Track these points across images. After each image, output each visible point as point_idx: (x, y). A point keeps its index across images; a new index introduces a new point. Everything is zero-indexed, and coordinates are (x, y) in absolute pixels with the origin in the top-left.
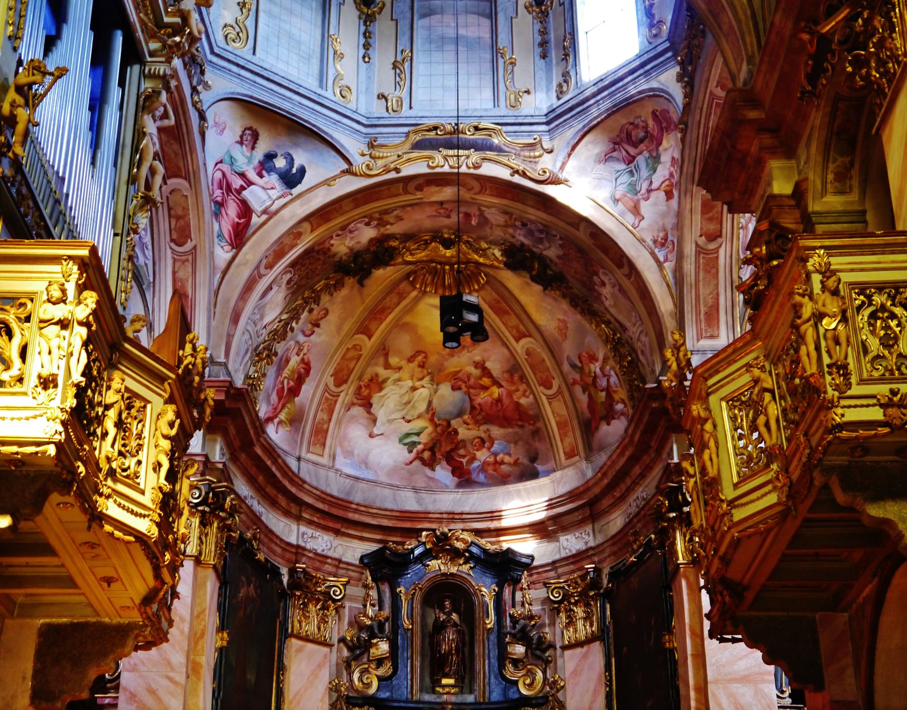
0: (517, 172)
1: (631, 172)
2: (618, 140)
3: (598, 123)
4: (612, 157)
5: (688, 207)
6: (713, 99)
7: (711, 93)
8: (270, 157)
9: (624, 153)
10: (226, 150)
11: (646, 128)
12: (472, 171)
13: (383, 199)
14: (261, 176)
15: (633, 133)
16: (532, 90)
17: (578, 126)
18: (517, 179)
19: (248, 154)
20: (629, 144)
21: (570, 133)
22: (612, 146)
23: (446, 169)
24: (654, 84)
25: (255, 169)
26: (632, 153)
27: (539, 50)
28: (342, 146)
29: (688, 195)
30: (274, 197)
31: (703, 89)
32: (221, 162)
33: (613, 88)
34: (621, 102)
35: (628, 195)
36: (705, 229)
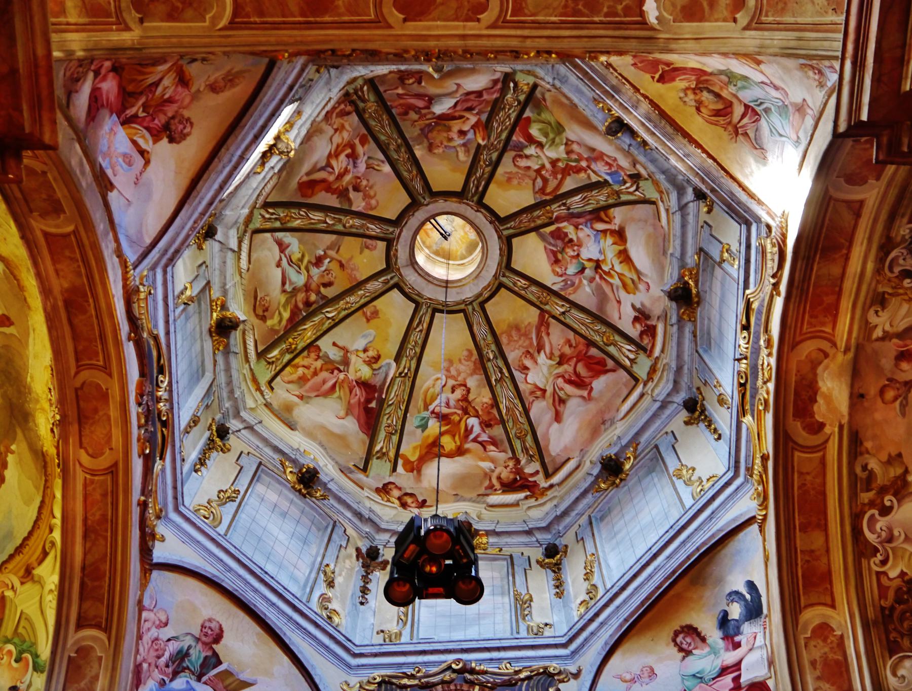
0: (776, 286)
1: (767, 110)
2: (730, 128)
4: (756, 139)
7: (493, 26)
8: (724, 621)
9: (745, 120)
10: (680, 679)
12: (775, 351)
13: (824, 484)
14: (737, 645)
15: (712, 107)
18: (783, 288)
19: (707, 650)
20: (731, 113)
22: (740, 138)
23: (771, 386)
25: (727, 650)
28: (734, 520)
30: (763, 642)
35: (791, 118)
36: (726, 13)
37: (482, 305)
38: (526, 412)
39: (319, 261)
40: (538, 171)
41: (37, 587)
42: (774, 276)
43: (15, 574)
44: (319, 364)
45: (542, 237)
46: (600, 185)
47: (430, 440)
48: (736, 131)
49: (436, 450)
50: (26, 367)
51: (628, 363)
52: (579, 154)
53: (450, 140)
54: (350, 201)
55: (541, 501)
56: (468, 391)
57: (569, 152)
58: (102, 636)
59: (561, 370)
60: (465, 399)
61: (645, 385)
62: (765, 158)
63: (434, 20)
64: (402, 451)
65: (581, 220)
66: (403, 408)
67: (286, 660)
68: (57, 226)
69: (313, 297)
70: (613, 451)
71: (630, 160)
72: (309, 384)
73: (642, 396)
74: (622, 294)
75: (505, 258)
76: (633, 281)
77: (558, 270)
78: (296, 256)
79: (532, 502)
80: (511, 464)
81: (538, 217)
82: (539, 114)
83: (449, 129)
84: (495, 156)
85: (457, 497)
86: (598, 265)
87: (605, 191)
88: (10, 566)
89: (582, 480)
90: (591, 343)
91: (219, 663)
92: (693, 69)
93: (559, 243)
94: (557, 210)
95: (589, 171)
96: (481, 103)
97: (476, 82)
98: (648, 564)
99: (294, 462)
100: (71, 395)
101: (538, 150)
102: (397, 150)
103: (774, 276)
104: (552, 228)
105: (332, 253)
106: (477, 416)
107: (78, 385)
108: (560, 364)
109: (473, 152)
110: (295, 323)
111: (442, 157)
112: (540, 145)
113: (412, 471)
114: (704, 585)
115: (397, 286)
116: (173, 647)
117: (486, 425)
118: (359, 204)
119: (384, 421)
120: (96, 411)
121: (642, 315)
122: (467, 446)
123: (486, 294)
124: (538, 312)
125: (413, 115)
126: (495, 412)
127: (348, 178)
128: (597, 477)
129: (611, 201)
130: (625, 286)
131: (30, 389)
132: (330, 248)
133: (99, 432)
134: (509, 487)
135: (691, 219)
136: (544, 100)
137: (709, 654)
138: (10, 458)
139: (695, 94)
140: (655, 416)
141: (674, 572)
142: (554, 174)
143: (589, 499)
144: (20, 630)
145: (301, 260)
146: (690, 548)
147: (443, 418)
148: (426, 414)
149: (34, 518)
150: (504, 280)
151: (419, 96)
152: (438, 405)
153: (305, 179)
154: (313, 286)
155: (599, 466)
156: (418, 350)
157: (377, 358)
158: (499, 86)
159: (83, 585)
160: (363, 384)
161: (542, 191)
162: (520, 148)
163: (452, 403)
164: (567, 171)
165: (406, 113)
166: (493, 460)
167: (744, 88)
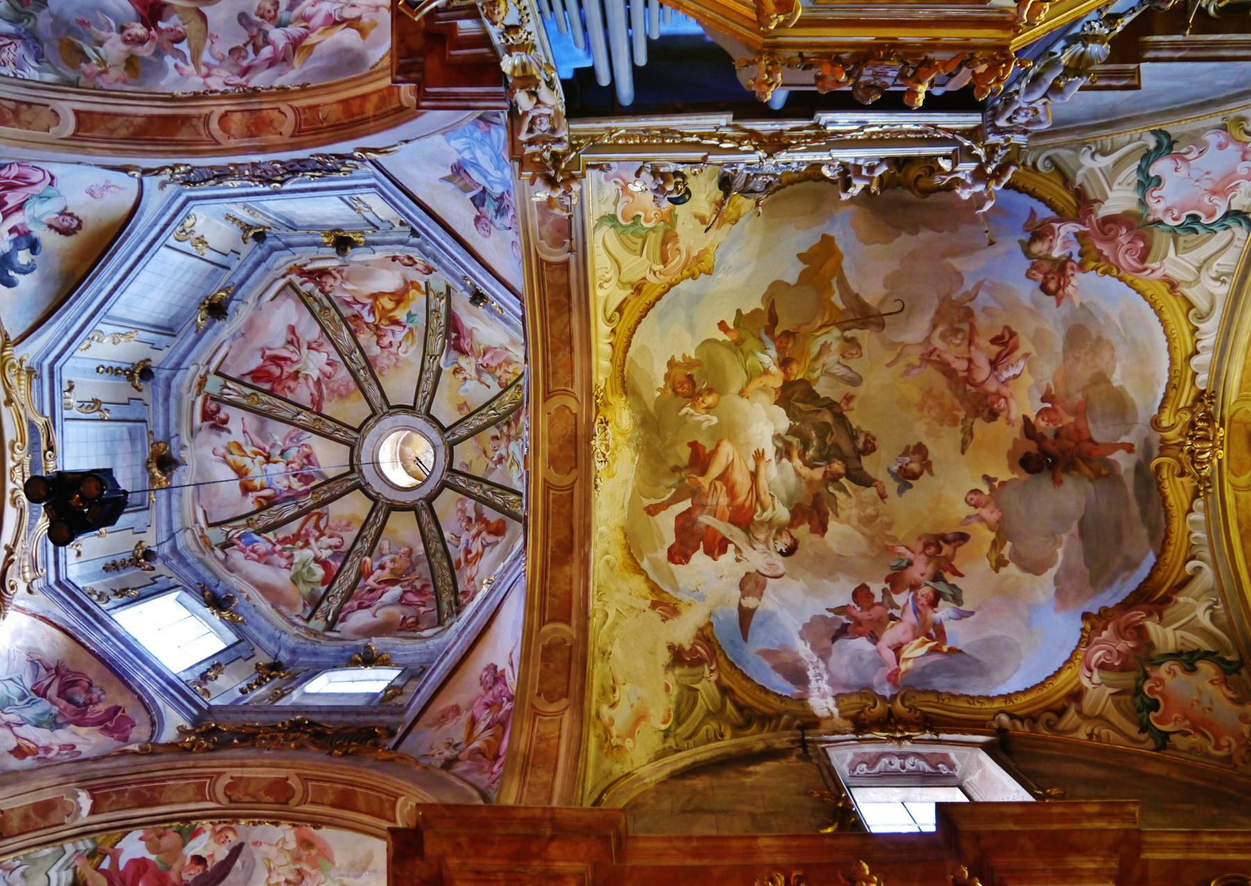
1: (24, 696)
2: (63, 672)
3: (83, 645)
4: (38, 668)
5: (45, 783)
6: (211, 778)
7: (220, 774)
8: (34, 246)
9: (47, 682)
10: (63, 193)
11: (91, 702)
12: (8, 496)
14: (11, 231)
15: (77, 689)
16: (82, 558)
17: (71, 620)
19: (45, 219)
20: (60, 686)
21: (58, 612)
22: (53, 665)
23: (10, 464)
24: (160, 702)
25: (23, 224)
26: (49, 693)
27: (109, 560)
28: (39, 336)
29: (61, 780)
31: (222, 762)
32: (51, 184)
33: (131, 655)
34: (120, 667)
37: (374, 414)
38: (323, 329)
39: (501, 459)
40: (322, 534)
41: (625, 280)
42: (13, 560)
43: (653, 285)
44: (498, 373)
45: (321, 475)
46: (268, 528)
47: (402, 305)
48: (57, 670)
49: (394, 298)
50: (638, 470)
51: (229, 384)
52: (281, 555)
53: (393, 561)
54: (476, 510)
55: (291, 264)
56: (378, 343)
57: (292, 556)
58: (543, 256)
59: (296, 367)
60: (380, 337)
61: (208, 372)
62: (29, 654)
63: (265, 779)
64: (424, 297)
65: (285, 495)
66: (430, 331)
67: (420, 196)
68: (555, 630)
69: (505, 429)
70: (218, 324)
71: (231, 561)
72: (503, 359)
73: (209, 363)
74: (241, 439)
75: (356, 453)
76: (231, 453)
77: (306, 450)
78: (515, 468)
79: (299, 263)
80: (327, 288)
81: (325, 492)
82: (313, 589)
83: (392, 570)
84: (359, 546)
85: (366, 264)
86: (268, 459)
87: (261, 524)
88: (660, 290)
89: (250, 294)
90: (270, 393)
91: (473, 199)
92: (85, 725)
93: (305, 472)
94: (308, 501)
95: (274, 540)
96: (361, 598)
97: (361, 618)
98: (121, 281)
99: (492, 310)
100: (582, 462)
101: (319, 554)
102: (436, 550)
103: (13, 560)
104: (313, 484)
105: (492, 465)
106: (367, 324)
107: (574, 473)
108: (297, 372)
109: (377, 549)
110: (517, 408)
111: (403, 544)
112: (316, 560)
113: (412, 283)
114: (61, 272)
115: (443, 430)
116: (507, 221)
117: (357, 317)
118: (470, 504)
119: (443, 321)
120: (561, 448)
121: (219, 426)
122: (370, 301)
123: (371, 422)
124: (324, 412)
125: (418, 584)
126: (352, 327)
127: (474, 531)
128: (231, 299)
129: (256, 517)
130: (239, 447)
131: (637, 449)
132: (493, 470)
133: (559, 429)
134: (323, 272)
135: (164, 527)
136: (305, 605)
137: (40, 217)
138: (661, 384)
139: (91, 699)
140: (184, 357)
141: (91, 281)
142: (307, 534)
143: (236, 280)
144: (640, 241)
145: (512, 464)
146: (80, 303)
147: (396, 322)
148: (410, 325)
149: (635, 336)
150: (355, 435)
151: (409, 604)
152: (400, 334)
153: (500, 538)
154: (505, 439)
155: (229, 311)
156: (424, 376)
157: (455, 372)
158: (341, 616)
159: (569, 296)
160: (463, 352)
161: (320, 516)
162: (335, 556)
163: (390, 334)
164: (297, 537)
165: (424, 586)
166: (345, 290)
167: (42, 715)
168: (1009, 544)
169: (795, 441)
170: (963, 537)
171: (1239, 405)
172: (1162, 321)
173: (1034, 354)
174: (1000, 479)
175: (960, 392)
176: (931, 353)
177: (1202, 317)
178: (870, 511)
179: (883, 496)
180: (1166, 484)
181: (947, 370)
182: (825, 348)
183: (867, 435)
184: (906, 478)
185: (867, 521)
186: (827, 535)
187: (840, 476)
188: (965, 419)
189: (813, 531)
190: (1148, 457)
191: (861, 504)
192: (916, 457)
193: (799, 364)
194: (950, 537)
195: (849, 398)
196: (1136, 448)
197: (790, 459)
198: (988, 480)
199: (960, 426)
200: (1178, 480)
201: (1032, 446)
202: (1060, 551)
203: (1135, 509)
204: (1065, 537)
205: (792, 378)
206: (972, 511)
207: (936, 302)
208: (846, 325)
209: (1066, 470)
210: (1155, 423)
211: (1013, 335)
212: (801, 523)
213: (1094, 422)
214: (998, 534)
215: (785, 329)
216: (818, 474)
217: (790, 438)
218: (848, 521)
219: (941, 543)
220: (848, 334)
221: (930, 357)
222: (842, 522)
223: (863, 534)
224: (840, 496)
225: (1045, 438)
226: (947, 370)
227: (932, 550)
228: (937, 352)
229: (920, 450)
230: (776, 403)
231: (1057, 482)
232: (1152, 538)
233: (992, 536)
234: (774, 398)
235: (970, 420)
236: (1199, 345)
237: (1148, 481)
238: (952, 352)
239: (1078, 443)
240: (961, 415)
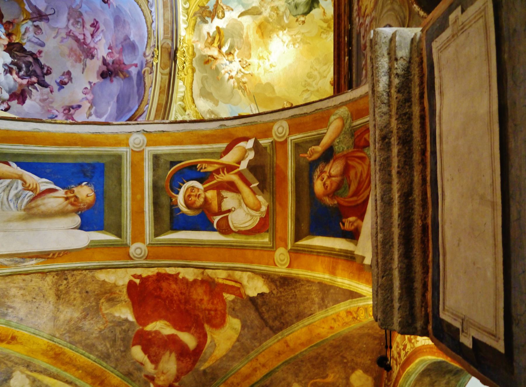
168: (94, 107)
169: (14, 67)
170: (79, 106)
171: (165, 41)
172: (142, 10)
173: (105, 30)
174: (94, 83)
175: (82, 48)
176: (70, 32)
177: (151, 6)
178: (45, 97)
179: (52, 92)
180: (146, 78)
181: (77, 40)
182: (27, 30)
183: (48, 67)
184: (62, 84)
185: (43, 100)
186: (24, 105)
187: (35, 83)
188: (84, 59)
189: (18, 103)
190: (142, 68)
191: (42, 94)
192: (67, 76)
193: (16, 36)
194: (75, 107)
195: (40, 52)
196: (138, 65)
197: (11, 74)
198: (90, 83)
199: (82, 63)
200: (149, 75)
201: (104, 68)
202: (109, 108)
203: (136, 89)
204: (112, 103)
205: (13, 42)
206: (84, 96)
207: (67, 9)
208: (34, 20)
209: (115, 76)
210: (144, 55)
211: (97, 22)
212: (14, 100)
213: (125, 56)
214: (91, 105)
215: (8, 20)
216: (25, 82)
217: (12, 66)
218: (35, 100)
219: (71, 109)
220: (36, 23)
221: (69, 34)
222: (32, 100)
223: (40, 105)
224: (34, 91)
225: (109, 64)
226: (77, 40)
227: (66, 111)
228: (72, 32)
229: (69, 73)
230: (4, 51)
231: (112, 81)
232: (139, 99)
233: (89, 105)
234: (3, 48)
235: (85, 60)
236: (154, 18)
237: (141, 76)
238: (77, 31)
239: (119, 65)
240: (82, 58)
